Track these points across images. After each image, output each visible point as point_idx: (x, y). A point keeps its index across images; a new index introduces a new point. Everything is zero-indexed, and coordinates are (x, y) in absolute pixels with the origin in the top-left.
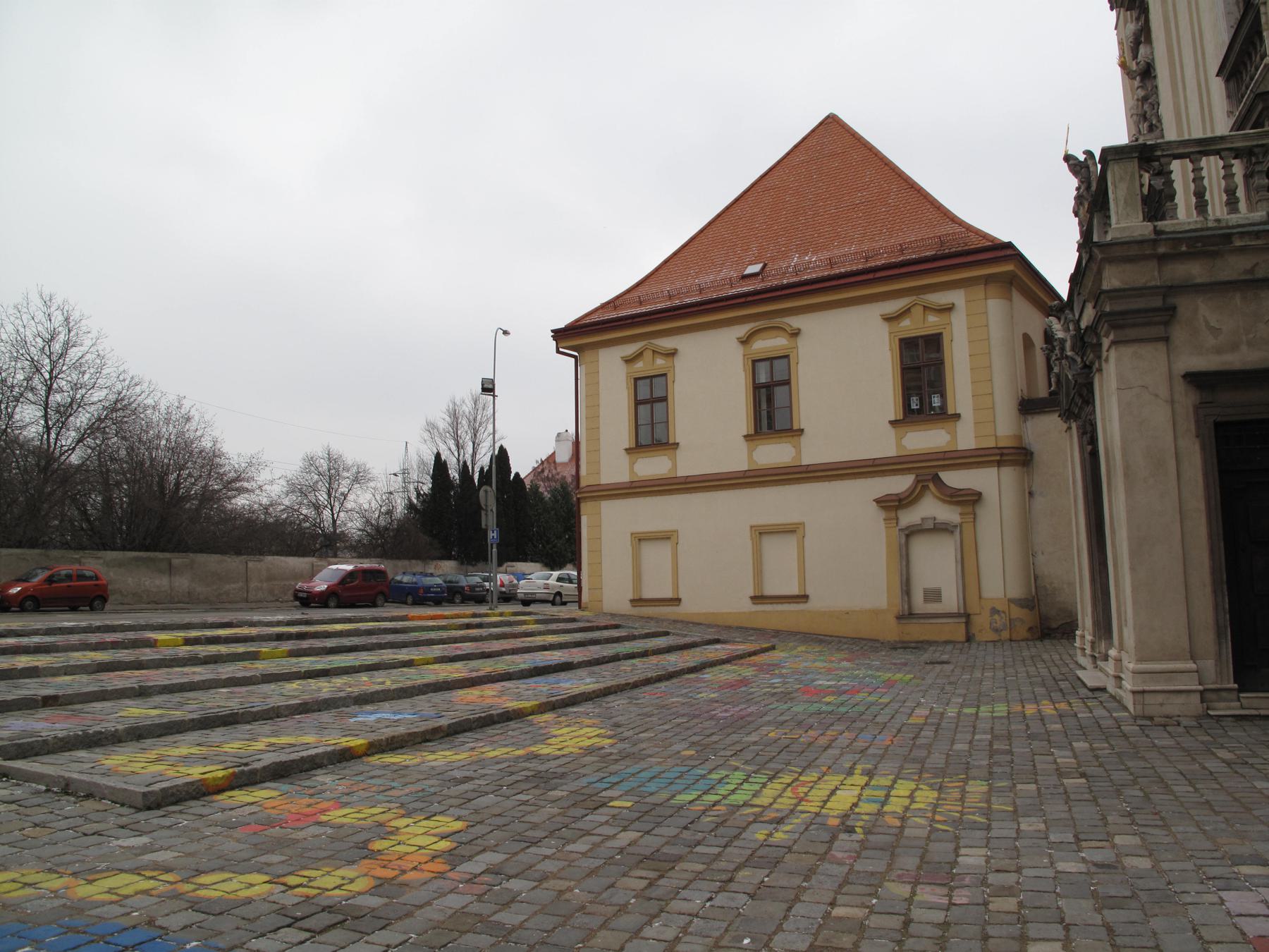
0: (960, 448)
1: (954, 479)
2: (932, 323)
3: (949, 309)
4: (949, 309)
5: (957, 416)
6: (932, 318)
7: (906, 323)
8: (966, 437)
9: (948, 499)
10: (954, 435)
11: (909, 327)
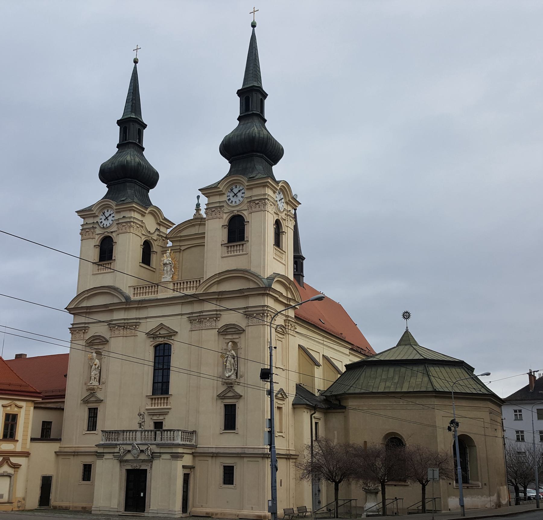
0: (17, 451)
1: (14, 460)
2: (15, 410)
3: (20, 407)
4: (20, 407)
5: (17, 441)
6: (16, 409)
7: (9, 408)
8: (18, 447)
9: (13, 466)
10: (15, 446)
11: (9, 410)
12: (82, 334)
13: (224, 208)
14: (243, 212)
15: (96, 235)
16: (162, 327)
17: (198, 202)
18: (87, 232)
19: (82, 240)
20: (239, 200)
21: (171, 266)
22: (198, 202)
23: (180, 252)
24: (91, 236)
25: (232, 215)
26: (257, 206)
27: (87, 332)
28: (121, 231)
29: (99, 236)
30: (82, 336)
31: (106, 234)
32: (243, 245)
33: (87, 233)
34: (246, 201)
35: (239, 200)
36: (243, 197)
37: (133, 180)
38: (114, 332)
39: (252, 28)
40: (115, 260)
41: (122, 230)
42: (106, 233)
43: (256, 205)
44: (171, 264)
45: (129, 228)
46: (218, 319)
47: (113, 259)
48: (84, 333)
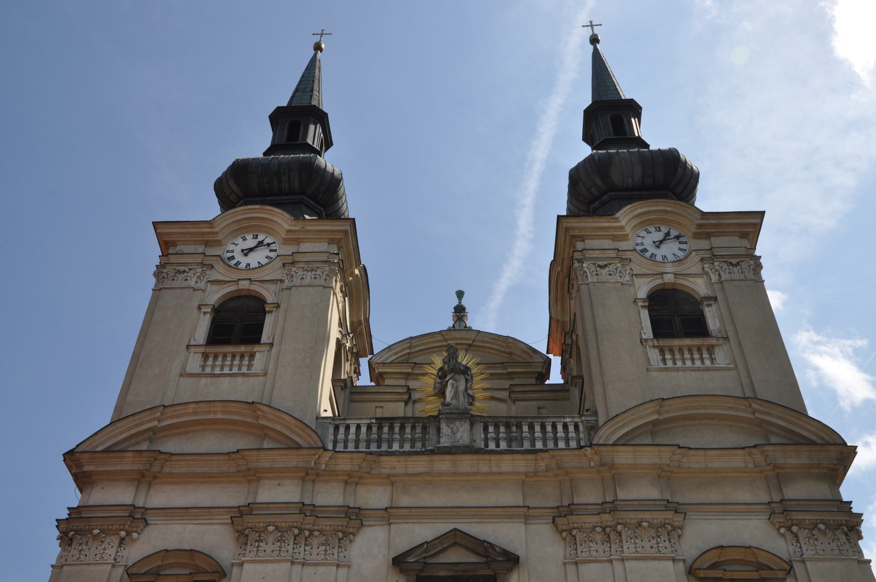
12: (116, 541)
13: (632, 265)
14: (691, 279)
15: (209, 284)
16: (456, 539)
17: (460, 302)
18: (179, 272)
19: (160, 289)
20: (674, 254)
21: (467, 381)
22: (460, 302)
23: (406, 403)
24: (192, 283)
25: (658, 282)
26: (735, 269)
27: (134, 541)
28: (296, 280)
29: (215, 287)
30: (112, 552)
31: (244, 285)
32: (711, 349)
33: (181, 276)
34: (698, 258)
35: (674, 254)
36: (686, 250)
37: (319, 207)
38: (259, 546)
39: (595, 33)
40: (271, 345)
41: (302, 278)
42: (244, 282)
43: (731, 267)
44: (468, 375)
45: (328, 278)
46: (679, 531)
47: (262, 342)
48: (122, 541)
